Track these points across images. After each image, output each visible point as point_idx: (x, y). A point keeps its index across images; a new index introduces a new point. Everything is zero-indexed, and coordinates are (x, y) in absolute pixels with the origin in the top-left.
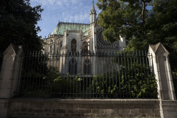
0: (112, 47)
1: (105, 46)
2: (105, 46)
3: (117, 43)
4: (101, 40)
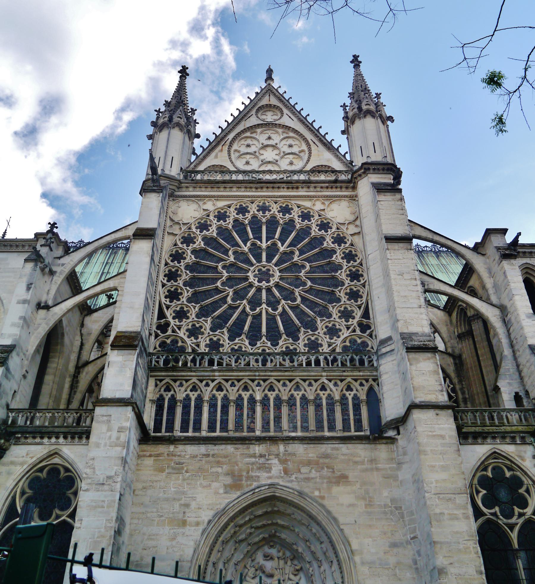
0: (313, 346)
1: (243, 342)
2: (243, 342)
3: (358, 314)
4: (207, 294)
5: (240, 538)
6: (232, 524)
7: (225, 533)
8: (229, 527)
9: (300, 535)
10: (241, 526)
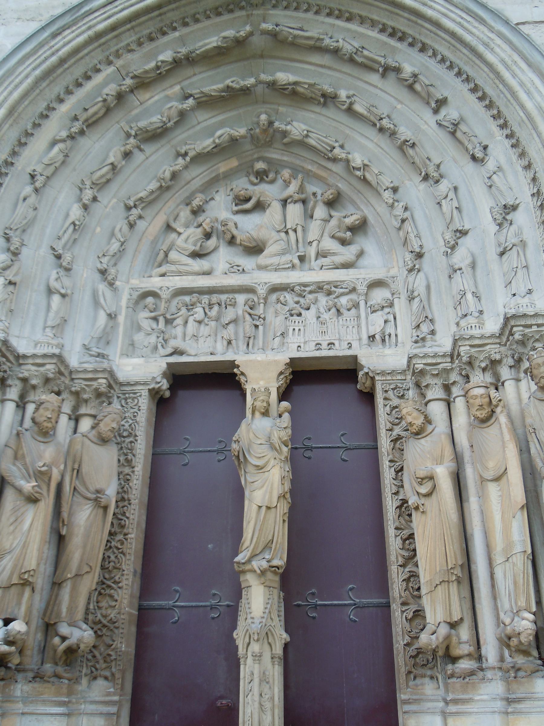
5: (142, 124)
6: (111, 69)
7: (80, 93)
8: (98, 79)
9: (358, 108)
10: (143, 83)
